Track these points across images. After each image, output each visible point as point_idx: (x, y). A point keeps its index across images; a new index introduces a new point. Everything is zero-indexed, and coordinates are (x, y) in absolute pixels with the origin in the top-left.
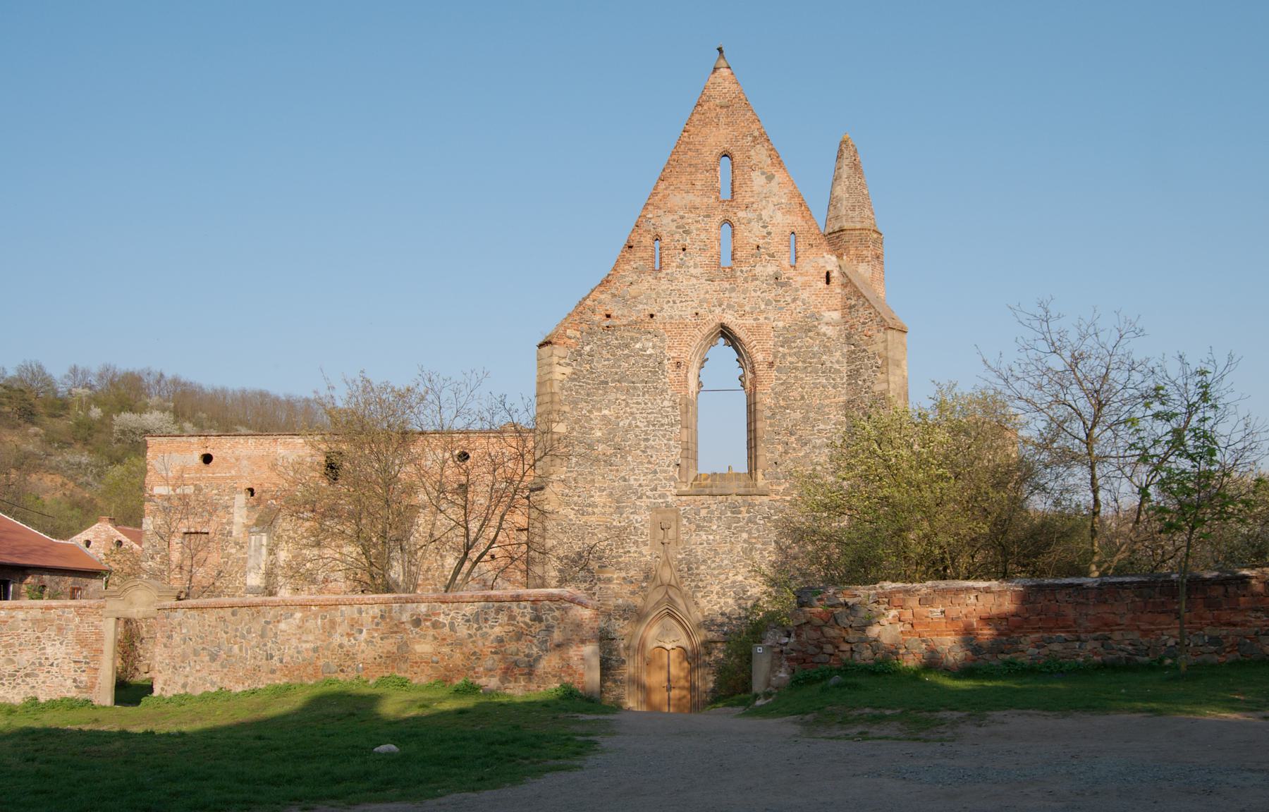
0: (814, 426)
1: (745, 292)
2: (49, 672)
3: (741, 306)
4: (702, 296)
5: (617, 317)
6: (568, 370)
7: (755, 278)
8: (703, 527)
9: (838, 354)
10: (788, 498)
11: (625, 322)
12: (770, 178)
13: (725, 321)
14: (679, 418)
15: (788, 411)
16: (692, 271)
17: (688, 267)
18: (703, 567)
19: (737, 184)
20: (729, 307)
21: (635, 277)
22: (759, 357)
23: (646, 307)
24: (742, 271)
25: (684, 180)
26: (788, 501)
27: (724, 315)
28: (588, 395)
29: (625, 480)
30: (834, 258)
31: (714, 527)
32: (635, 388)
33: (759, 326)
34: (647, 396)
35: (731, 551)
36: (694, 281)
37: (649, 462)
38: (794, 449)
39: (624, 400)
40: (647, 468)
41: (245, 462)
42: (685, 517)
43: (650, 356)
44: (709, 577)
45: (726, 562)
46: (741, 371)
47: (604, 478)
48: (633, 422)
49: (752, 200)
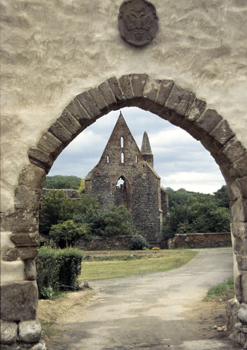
3: (126, 172)
7: (129, 166)
12: (132, 143)
13: (123, 175)
20: (124, 172)
32: (104, 190)
36: (116, 166)
43: (107, 183)
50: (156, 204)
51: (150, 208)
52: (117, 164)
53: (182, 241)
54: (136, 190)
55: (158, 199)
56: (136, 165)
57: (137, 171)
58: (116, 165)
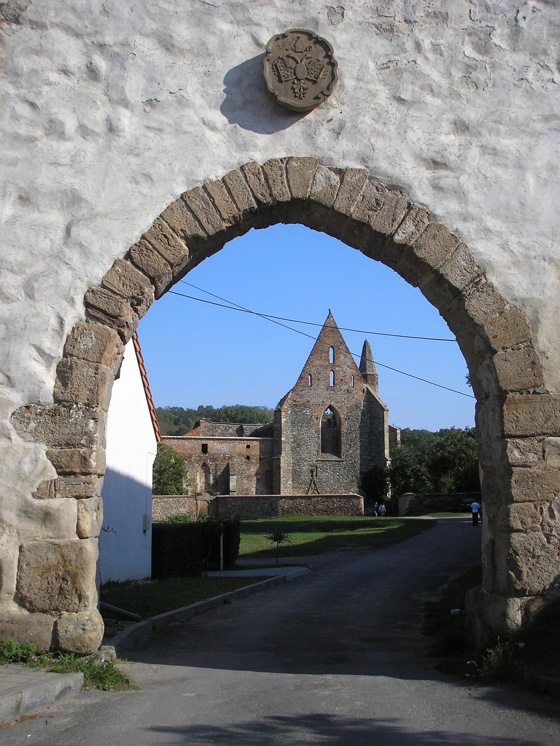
16: (322, 387)
19: (335, 358)
20: (333, 400)
22: (342, 416)
25: (318, 356)
33: (342, 406)
51: (373, 454)
57: (353, 398)
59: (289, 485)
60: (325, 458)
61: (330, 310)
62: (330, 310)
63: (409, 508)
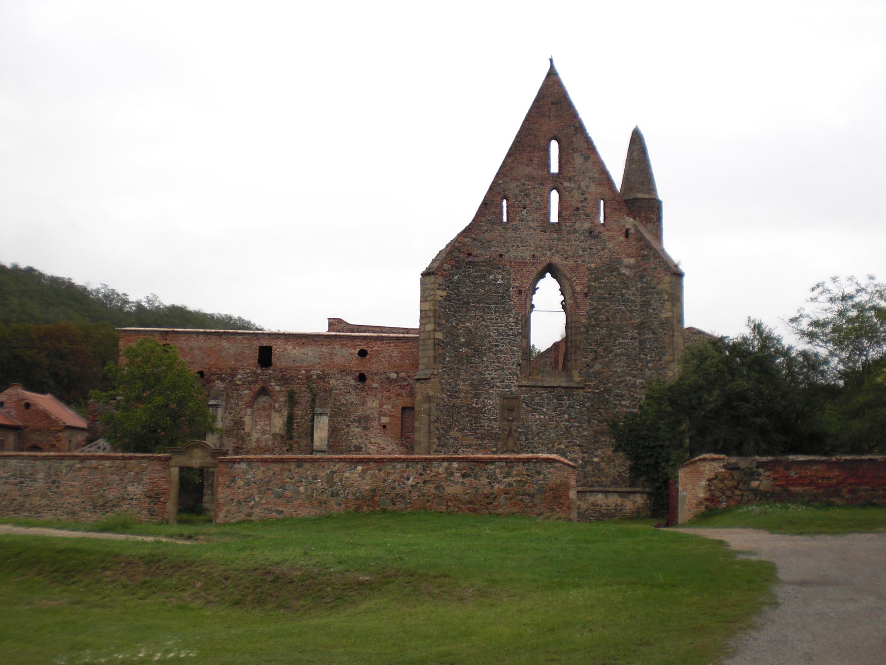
0: (616, 340)
1: (568, 241)
2: (130, 504)
3: (566, 251)
4: (537, 243)
5: (477, 254)
6: (444, 294)
7: (575, 231)
8: (537, 409)
9: (634, 288)
10: (597, 391)
11: (482, 259)
13: (553, 262)
14: (520, 331)
15: (598, 329)
16: (531, 224)
17: (528, 221)
18: (536, 438)
20: (557, 252)
21: (489, 227)
22: (578, 289)
23: (497, 249)
24: (566, 226)
26: (597, 393)
27: (553, 257)
28: (456, 312)
29: (481, 374)
30: (631, 220)
31: (545, 410)
32: (489, 308)
33: (578, 266)
34: (497, 314)
35: (556, 427)
36: (532, 231)
37: (499, 362)
38: (602, 356)
39: (481, 316)
40: (497, 366)
41: (197, 352)
42: (524, 402)
44: (541, 445)
45: (553, 435)
46: (562, 298)
47: (466, 372)
48: (488, 333)
49: (574, 174)
50: (667, 358)
52: (534, 224)
53: (736, 488)
54: (598, 311)
55: (673, 342)
56: (601, 229)
58: (530, 227)
59: (451, 441)
60: (538, 380)
61: (551, 60)
62: (551, 60)
63: (706, 499)
